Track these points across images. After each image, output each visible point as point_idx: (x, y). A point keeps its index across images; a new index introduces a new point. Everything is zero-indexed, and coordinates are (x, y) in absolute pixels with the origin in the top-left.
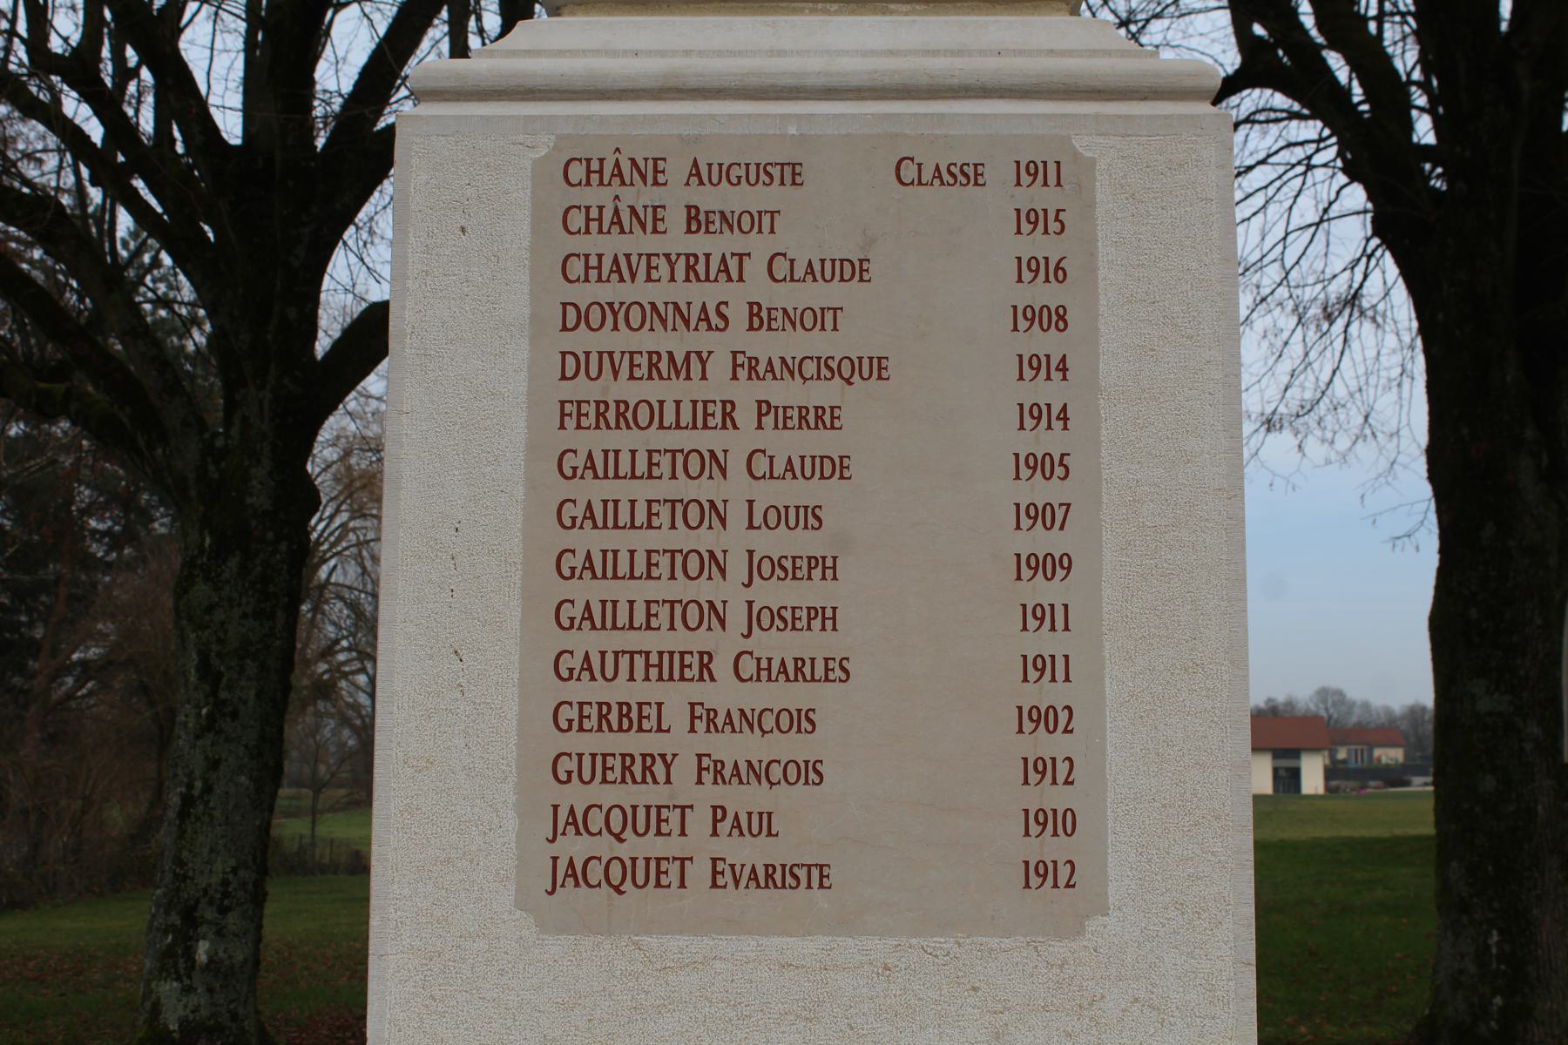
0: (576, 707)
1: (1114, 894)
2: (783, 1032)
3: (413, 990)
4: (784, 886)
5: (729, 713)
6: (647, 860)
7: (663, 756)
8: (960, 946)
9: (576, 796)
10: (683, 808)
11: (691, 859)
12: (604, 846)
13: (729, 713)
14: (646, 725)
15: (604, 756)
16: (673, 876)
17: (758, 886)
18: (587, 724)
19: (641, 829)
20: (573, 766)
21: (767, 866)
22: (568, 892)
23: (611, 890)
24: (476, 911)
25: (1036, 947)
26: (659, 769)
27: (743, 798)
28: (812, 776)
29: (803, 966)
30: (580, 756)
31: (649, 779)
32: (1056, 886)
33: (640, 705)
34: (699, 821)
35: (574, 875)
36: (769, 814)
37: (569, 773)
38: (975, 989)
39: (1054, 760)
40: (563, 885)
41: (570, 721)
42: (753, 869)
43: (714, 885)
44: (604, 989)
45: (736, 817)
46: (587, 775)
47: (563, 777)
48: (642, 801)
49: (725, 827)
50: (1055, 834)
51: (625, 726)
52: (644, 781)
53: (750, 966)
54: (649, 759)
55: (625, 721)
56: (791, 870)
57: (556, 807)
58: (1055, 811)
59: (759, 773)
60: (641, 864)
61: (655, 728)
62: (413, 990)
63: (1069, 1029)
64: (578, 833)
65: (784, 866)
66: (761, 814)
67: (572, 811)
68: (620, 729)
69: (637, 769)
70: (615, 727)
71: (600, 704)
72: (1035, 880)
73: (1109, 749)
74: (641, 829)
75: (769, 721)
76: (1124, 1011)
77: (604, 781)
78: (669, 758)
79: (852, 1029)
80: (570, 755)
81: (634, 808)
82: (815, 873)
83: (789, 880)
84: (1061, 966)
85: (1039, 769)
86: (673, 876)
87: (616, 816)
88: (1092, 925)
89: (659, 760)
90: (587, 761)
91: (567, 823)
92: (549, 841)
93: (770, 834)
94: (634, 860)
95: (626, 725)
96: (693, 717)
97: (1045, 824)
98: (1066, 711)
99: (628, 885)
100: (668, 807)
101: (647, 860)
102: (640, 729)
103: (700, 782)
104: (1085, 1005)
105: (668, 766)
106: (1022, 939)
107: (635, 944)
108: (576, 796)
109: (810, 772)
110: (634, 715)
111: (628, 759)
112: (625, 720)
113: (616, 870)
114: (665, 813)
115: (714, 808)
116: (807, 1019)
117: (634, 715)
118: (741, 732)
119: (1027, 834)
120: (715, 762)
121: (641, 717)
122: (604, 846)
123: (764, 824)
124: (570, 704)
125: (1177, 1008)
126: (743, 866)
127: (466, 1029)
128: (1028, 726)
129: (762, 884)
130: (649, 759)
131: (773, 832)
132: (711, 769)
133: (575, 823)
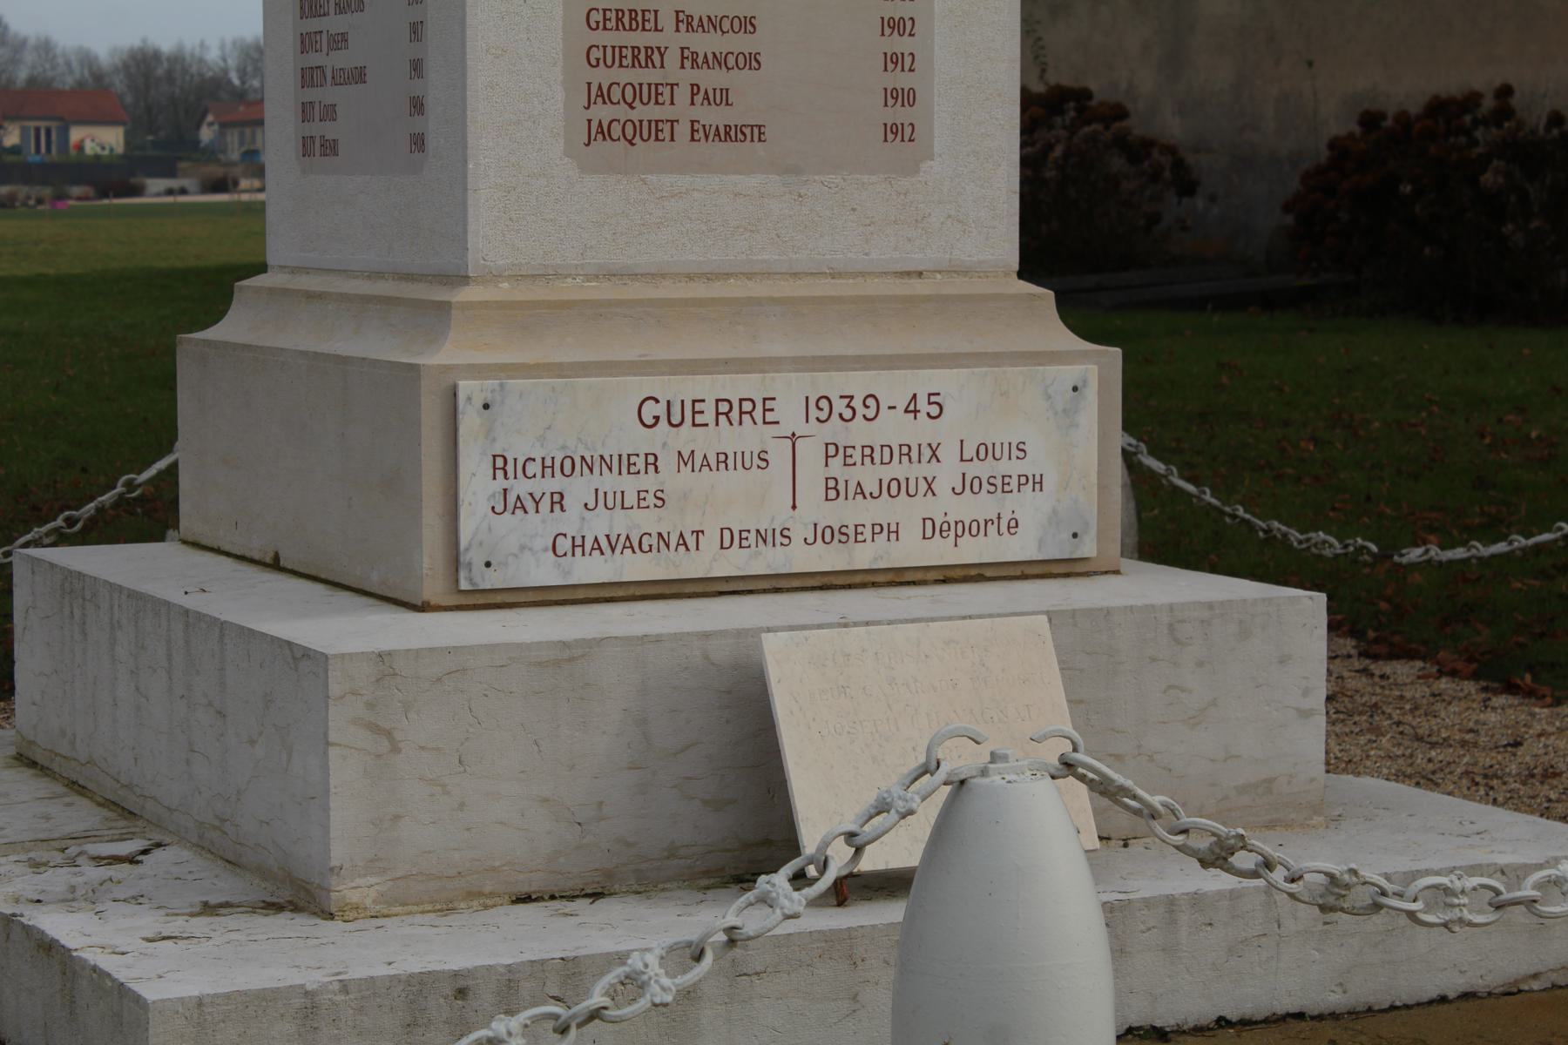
0: (601, 12)
1: (937, 149)
2: (736, 240)
3: (498, 214)
4: (736, 140)
5: (701, 19)
6: (650, 122)
7: (659, 48)
8: (844, 180)
9: (603, 76)
10: (672, 85)
11: (677, 121)
12: (622, 112)
13: (701, 19)
14: (647, 26)
15: (621, 48)
16: (666, 134)
17: (720, 140)
18: (609, 25)
19: (645, 100)
20: (600, 55)
21: (726, 126)
22: (599, 145)
23: (626, 143)
24: (538, 158)
25: (890, 182)
26: (656, 57)
27: (711, 79)
28: (754, 64)
29: (748, 195)
30: (605, 47)
31: (650, 65)
32: (903, 140)
33: (643, 11)
34: (683, 94)
35: (602, 132)
36: (727, 90)
37: (598, 60)
38: (854, 210)
39: (903, 54)
40: (595, 140)
41: (598, 23)
42: (717, 128)
43: (693, 139)
44: (623, 212)
45: (706, 92)
46: (609, 62)
47: (594, 62)
48: (645, 81)
49: (699, 98)
50: (903, 105)
51: (634, 27)
52: (647, 66)
53: (716, 195)
54: (649, 51)
55: (634, 22)
56: (740, 129)
57: (589, 84)
58: (903, 89)
59: (720, 61)
60: (645, 124)
61: (653, 29)
62: (498, 214)
63: (909, 236)
64: (604, 103)
65: (736, 126)
66: (722, 90)
67: (600, 87)
68: (631, 29)
69: (642, 57)
70: (627, 27)
71: (617, 11)
72: (890, 136)
73: (936, 48)
74: (645, 100)
75: (726, 25)
76: (942, 223)
77: (621, 65)
78: (663, 50)
79: (779, 237)
80: (598, 47)
81: (641, 85)
82: (756, 130)
83: (740, 136)
84: (905, 194)
85: (894, 61)
86: (666, 134)
87: (629, 91)
88: (924, 166)
89: (656, 51)
90: (609, 51)
91: (597, 96)
92: (585, 108)
93: (727, 104)
94: (641, 121)
95: (634, 27)
96: (678, 21)
97: (897, 99)
98: (911, 21)
99: (637, 140)
100: (662, 84)
101: (650, 122)
102: (644, 29)
103: (683, 67)
104: (919, 219)
105: (662, 56)
106: (882, 176)
107: (643, 180)
108: (603, 76)
109: (752, 61)
110: (639, 18)
111: (636, 50)
112: (634, 22)
113: (629, 129)
114: (660, 89)
115: (692, 85)
116: (751, 231)
117: (639, 18)
118: (709, 32)
119: (886, 105)
120: (692, 53)
121: (644, 20)
122: (622, 112)
123: (722, 97)
124: (598, 10)
125: (973, 221)
126: (711, 126)
127: (533, 241)
128: (887, 31)
129: (723, 139)
130: (649, 51)
131: (730, 103)
132: (689, 58)
133: (602, 96)
